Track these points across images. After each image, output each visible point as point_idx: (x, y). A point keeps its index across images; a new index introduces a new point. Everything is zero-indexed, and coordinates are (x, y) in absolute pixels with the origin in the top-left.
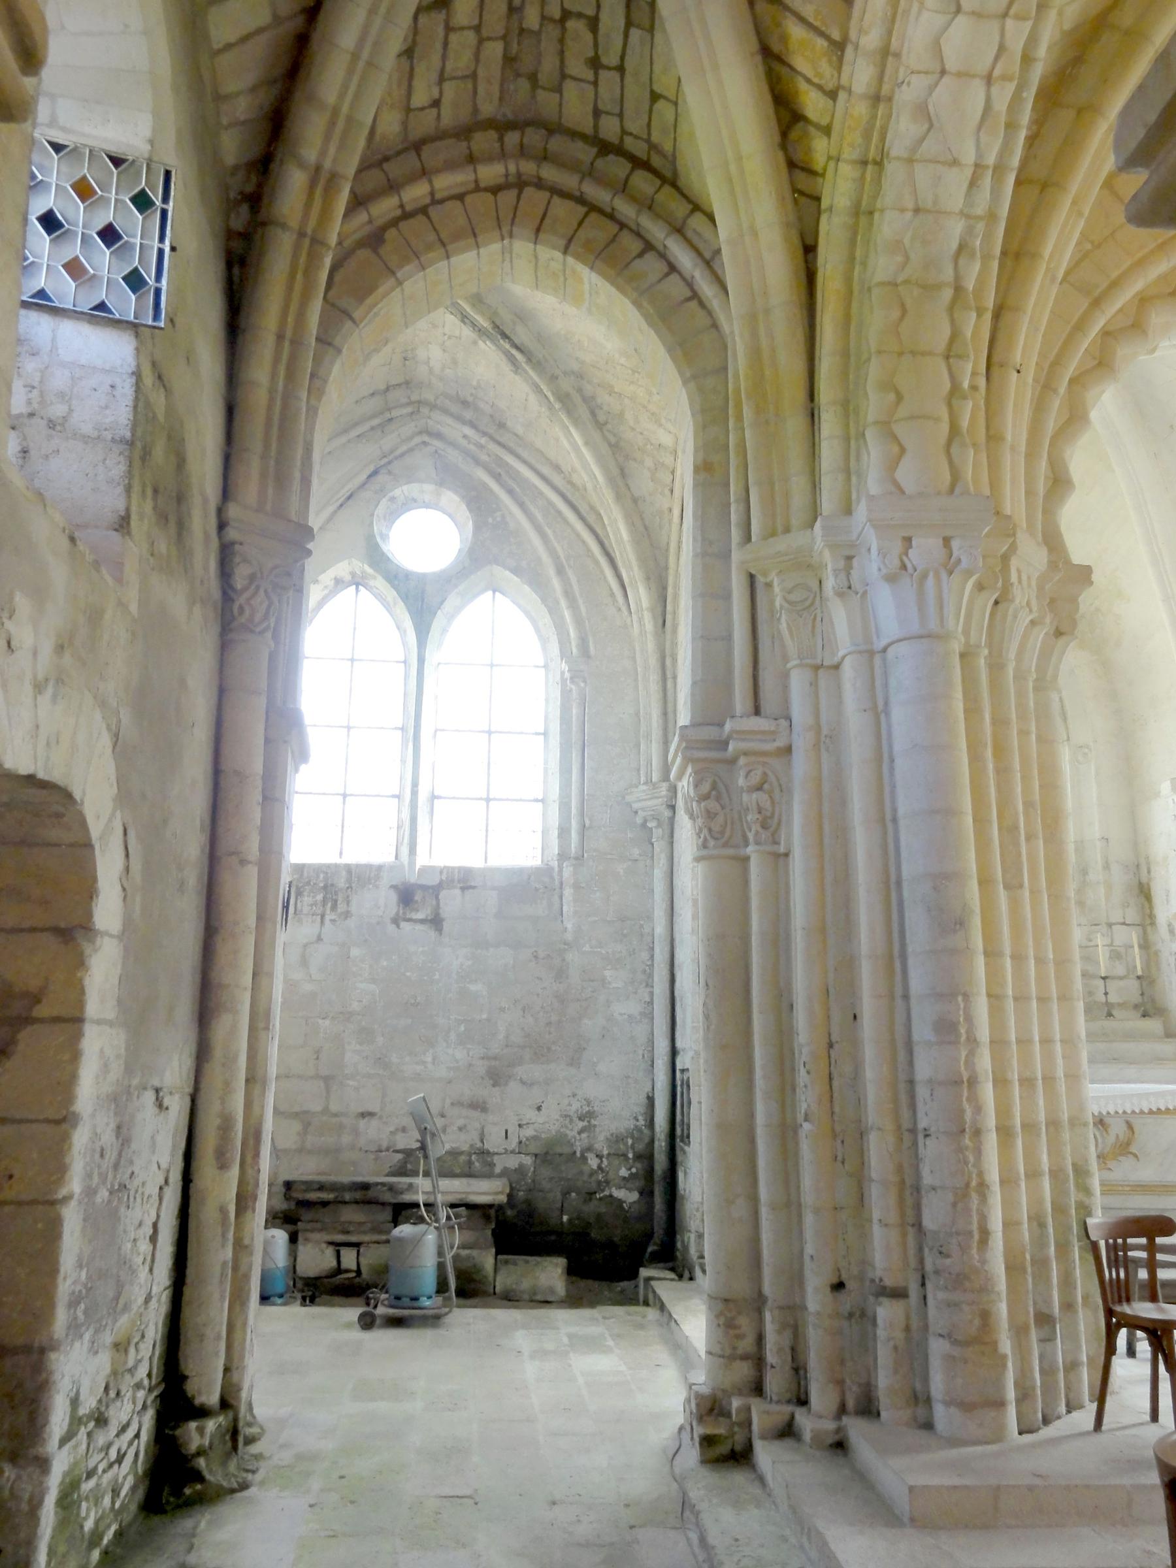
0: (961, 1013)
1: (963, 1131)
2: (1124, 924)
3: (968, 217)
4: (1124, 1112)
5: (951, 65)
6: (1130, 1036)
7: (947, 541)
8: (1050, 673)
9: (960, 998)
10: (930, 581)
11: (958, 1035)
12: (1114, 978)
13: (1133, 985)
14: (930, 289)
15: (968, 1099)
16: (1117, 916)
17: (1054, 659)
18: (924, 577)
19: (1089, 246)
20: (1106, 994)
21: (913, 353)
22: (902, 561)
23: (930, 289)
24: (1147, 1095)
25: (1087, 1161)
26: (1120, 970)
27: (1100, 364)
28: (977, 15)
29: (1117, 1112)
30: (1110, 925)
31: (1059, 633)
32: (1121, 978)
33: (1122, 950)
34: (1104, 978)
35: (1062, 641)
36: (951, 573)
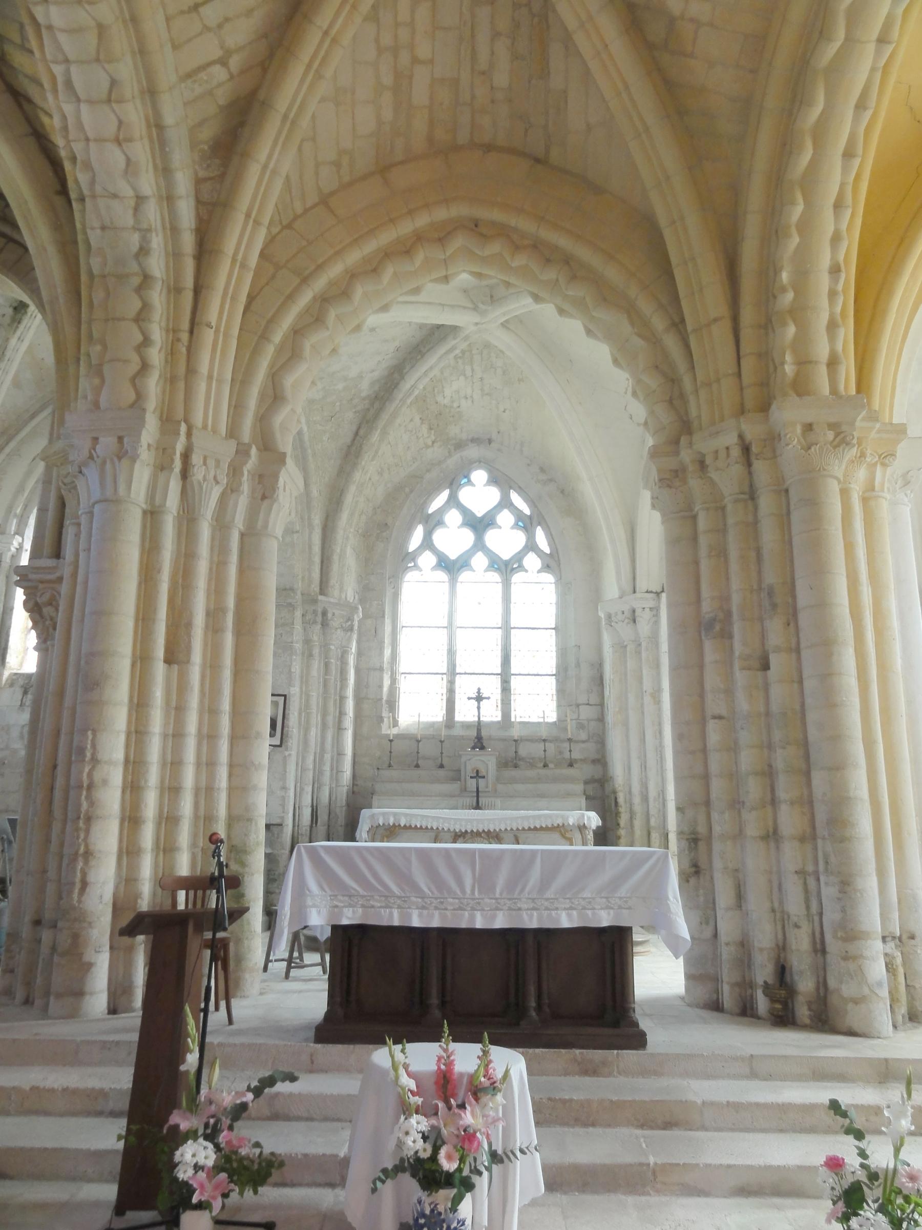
0: (89, 742)
1: (79, 818)
2: (588, 704)
3: (139, 230)
4: (512, 829)
5: (91, 135)
6: (556, 780)
7: (120, 439)
8: (260, 523)
9: (90, 733)
10: (108, 466)
11: (85, 756)
12: (577, 742)
13: (591, 747)
14: (122, 278)
15: (87, 798)
16: (583, 699)
17: (262, 516)
18: (104, 462)
19: (304, 243)
20: (570, 751)
21: (113, 319)
22: (90, 452)
23: (122, 278)
24: (527, 818)
25: (245, 844)
26: (583, 736)
27: (317, 320)
28: (90, 102)
29: (506, 830)
30: (578, 706)
31: (264, 497)
32: (583, 742)
33: (586, 723)
34: (544, 740)
35: (266, 502)
36: (120, 458)
